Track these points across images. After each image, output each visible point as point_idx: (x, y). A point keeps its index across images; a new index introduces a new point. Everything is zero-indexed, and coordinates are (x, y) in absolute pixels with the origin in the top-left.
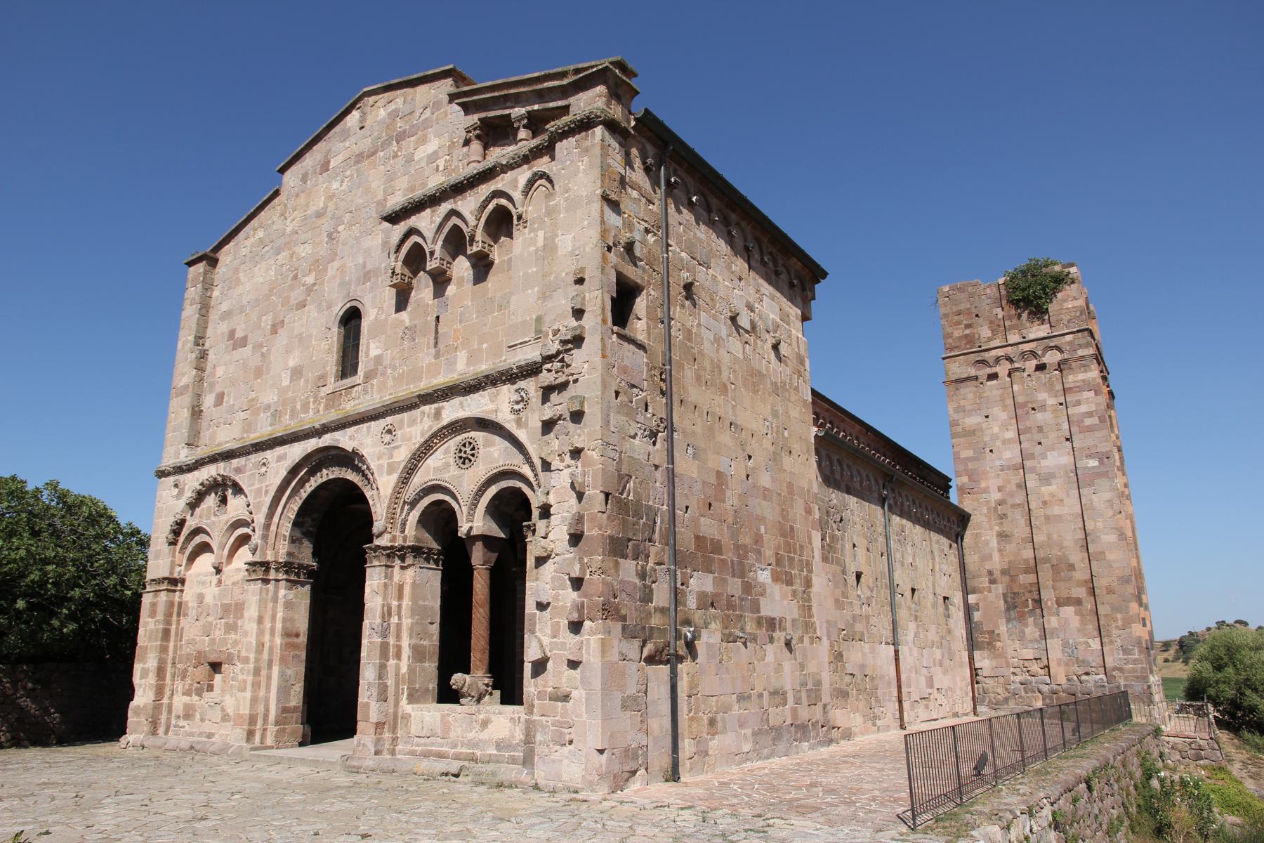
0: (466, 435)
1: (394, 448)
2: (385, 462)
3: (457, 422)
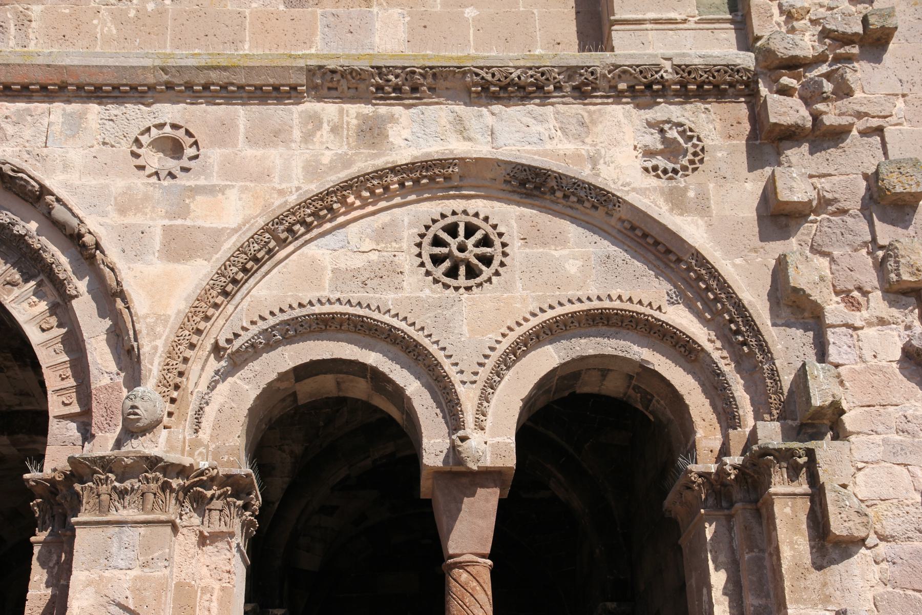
0: (458, 205)
1: (195, 191)
2: (156, 224)
3: (443, 163)
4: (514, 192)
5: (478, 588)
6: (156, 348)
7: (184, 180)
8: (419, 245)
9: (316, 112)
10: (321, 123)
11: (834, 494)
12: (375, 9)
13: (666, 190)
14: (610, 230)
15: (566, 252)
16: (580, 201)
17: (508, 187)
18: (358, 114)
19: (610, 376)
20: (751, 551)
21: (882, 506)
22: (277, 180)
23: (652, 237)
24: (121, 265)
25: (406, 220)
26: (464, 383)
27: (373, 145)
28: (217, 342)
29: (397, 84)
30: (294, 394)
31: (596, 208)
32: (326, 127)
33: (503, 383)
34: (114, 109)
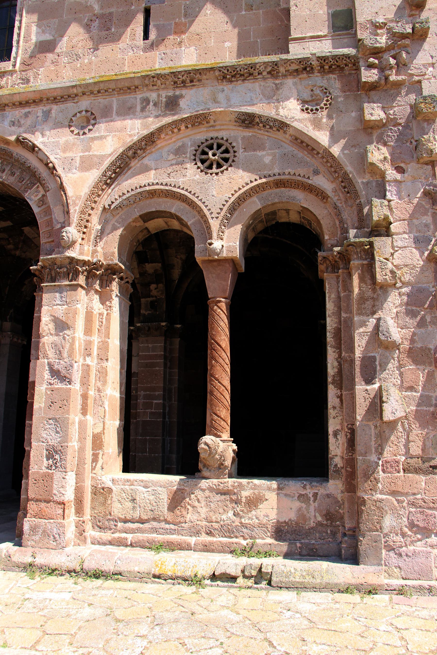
1: (93, 139)
4: (240, 126)
5: (221, 312)
6: (76, 210)
7: (89, 135)
8: (195, 155)
9: (147, 97)
10: (149, 102)
11: (379, 263)
12: (183, 48)
13: (312, 119)
14: (286, 141)
15: (264, 153)
16: (271, 128)
17: (238, 124)
18: (166, 96)
19: (291, 213)
20: (345, 292)
21: (405, 269)
22: (129, 130)
23: (305, 143)
24: (63, 175)
25: (189, 144)
26: (212, 218)
27: (172, 110)
28: (104, 206)
29: (183, 80)
30: (146, 228)
31: (279, 131)
32: (151, 104)
33: (233, 217)
34: (62, 106)
